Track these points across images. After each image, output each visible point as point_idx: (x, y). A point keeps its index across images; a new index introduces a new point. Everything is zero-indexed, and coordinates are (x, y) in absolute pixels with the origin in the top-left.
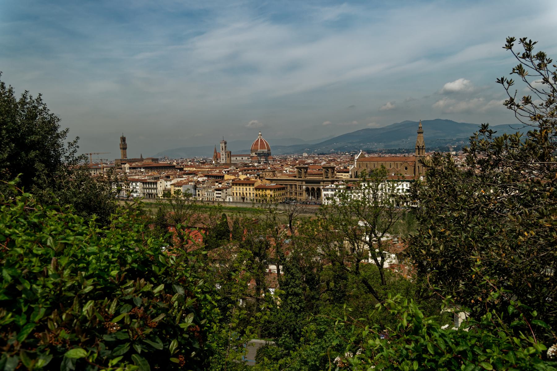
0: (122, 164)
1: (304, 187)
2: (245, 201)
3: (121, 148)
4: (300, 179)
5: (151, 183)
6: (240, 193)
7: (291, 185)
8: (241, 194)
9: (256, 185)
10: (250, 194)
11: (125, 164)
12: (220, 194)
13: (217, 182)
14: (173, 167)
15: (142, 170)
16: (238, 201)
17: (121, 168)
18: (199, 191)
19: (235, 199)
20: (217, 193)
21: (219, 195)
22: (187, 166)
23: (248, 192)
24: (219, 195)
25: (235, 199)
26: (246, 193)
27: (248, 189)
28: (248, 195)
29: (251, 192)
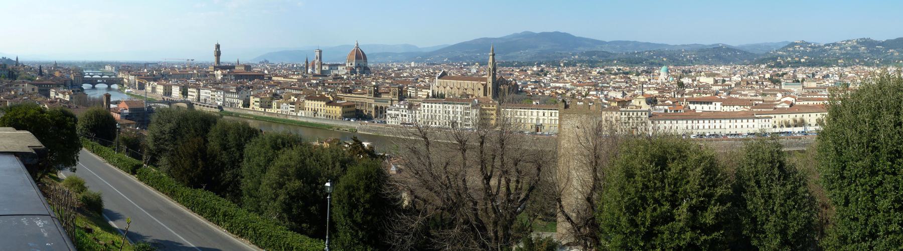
15: (233, 78)
22: (276, 76)
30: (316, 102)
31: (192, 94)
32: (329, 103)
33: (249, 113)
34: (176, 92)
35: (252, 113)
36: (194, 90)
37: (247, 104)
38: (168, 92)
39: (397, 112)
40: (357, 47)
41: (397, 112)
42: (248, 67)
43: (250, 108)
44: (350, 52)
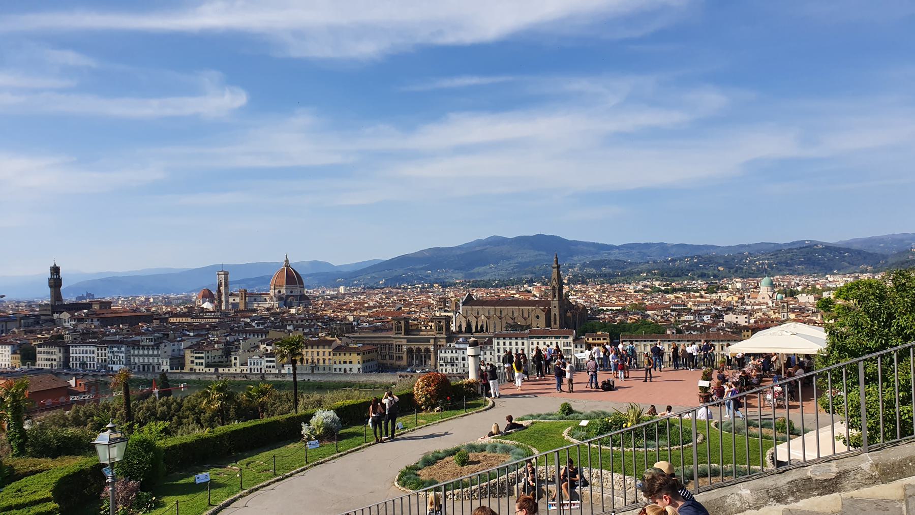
0: (53, 313)
1: (405, 348)
3: (50, 286)
7: (384, 345)
8: (310, 361)
9: (334, 345)
10: (324, 360)
11: (61, 312)
12: (273, 361)
13: (262, 342)
17: (53, 321)
18: (235, 359)
20: (268, 361)
21: (272, 364)
23: (321, 358)
26: (318, 360)
27: (321, 354)
28: (321, 362)
29: (327, 358)
33: (187, 377)
35: (193, 377)
36: (55, 350)
39: (455, 355)
40: (288, 266)
42: (106, 305)
43: (186, 370)
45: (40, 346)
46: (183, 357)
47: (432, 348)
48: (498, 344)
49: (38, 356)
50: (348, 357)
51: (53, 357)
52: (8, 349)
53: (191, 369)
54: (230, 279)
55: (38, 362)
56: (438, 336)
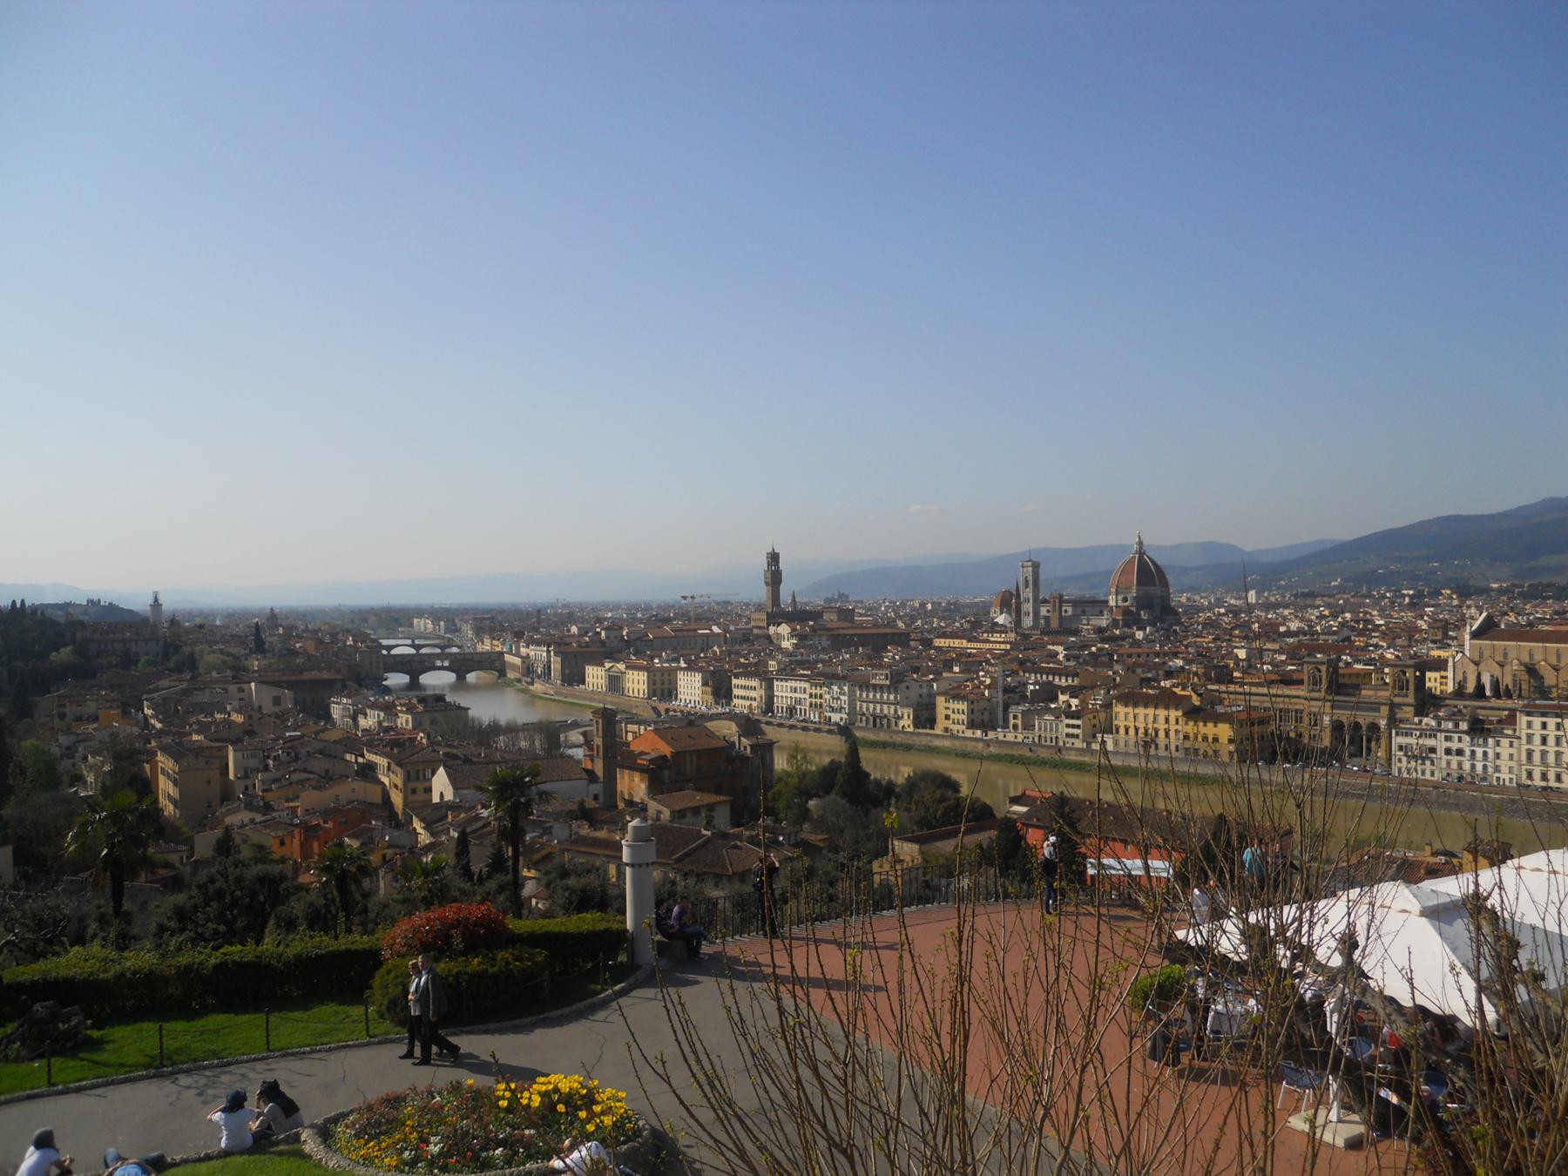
2: (1152, 751)
4: (1316, 695)
5: (882, 687)
6: (1137, 729)
8: (1141, 731)
12: (1078, 727)
14: (901, 639)
15: (826, 643)
16: (1132, 750)
17: (769, 637)
18: (1015, 717)
19: (1122, 743)
20: (1068, 726)
21: (1076, 731)
22: (944, 635)
24: (1076, 731)
25: (1122, 743)
28: (1162, 734)
30: (1151, 711)
31: (746, 694)
32: (1193, 714)
33: (937, 743)
34: (691, 689)
35: (947, 743)
36: (755, 683)
37: (925, 717)
38: (663, 688)
39: (1430, 742)
40: (1141, 553)
41: (1430, 742)
43: (938, 730)
44: (1119, 566)
45: (737, 677)
46: (933, 706)
47: (1383, 723)
48: (1529, 725)
49: (736, 692)
50: (1209, 729)
51: (753, 694)
52: (699, 677)
53: (946, 730)
54: (1042, 576)
55: (735, 701)
56: (1397, 700)
